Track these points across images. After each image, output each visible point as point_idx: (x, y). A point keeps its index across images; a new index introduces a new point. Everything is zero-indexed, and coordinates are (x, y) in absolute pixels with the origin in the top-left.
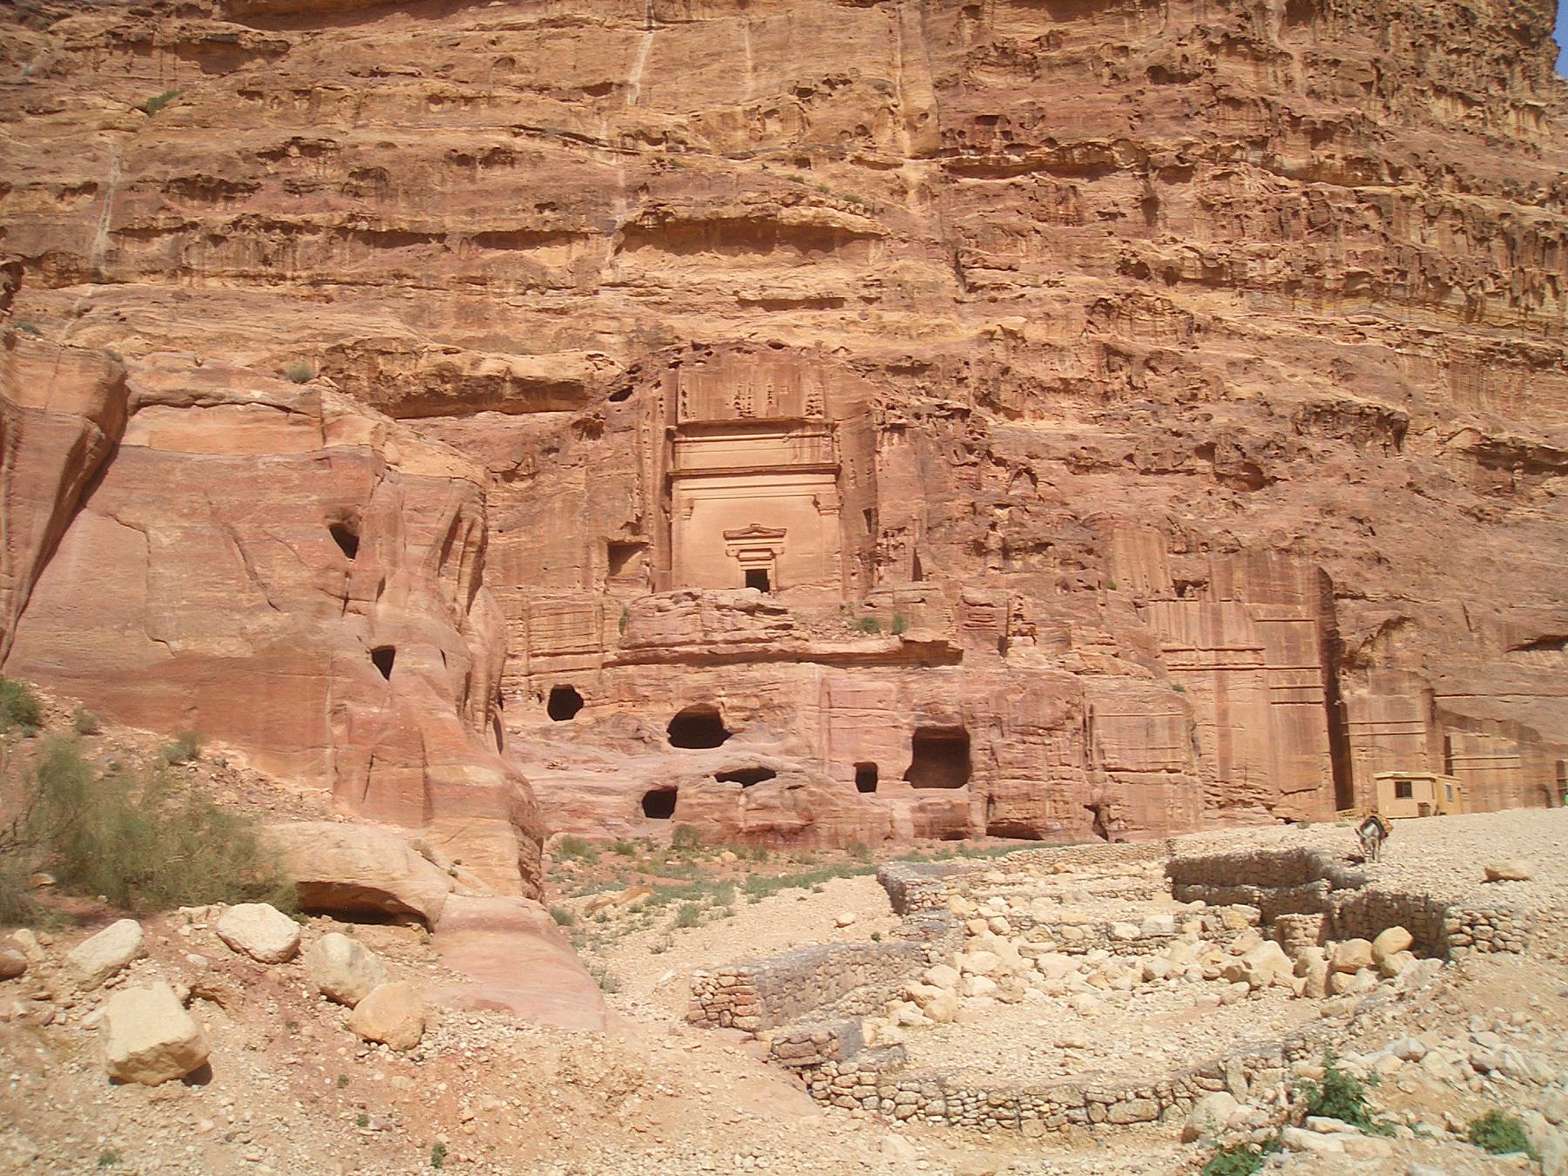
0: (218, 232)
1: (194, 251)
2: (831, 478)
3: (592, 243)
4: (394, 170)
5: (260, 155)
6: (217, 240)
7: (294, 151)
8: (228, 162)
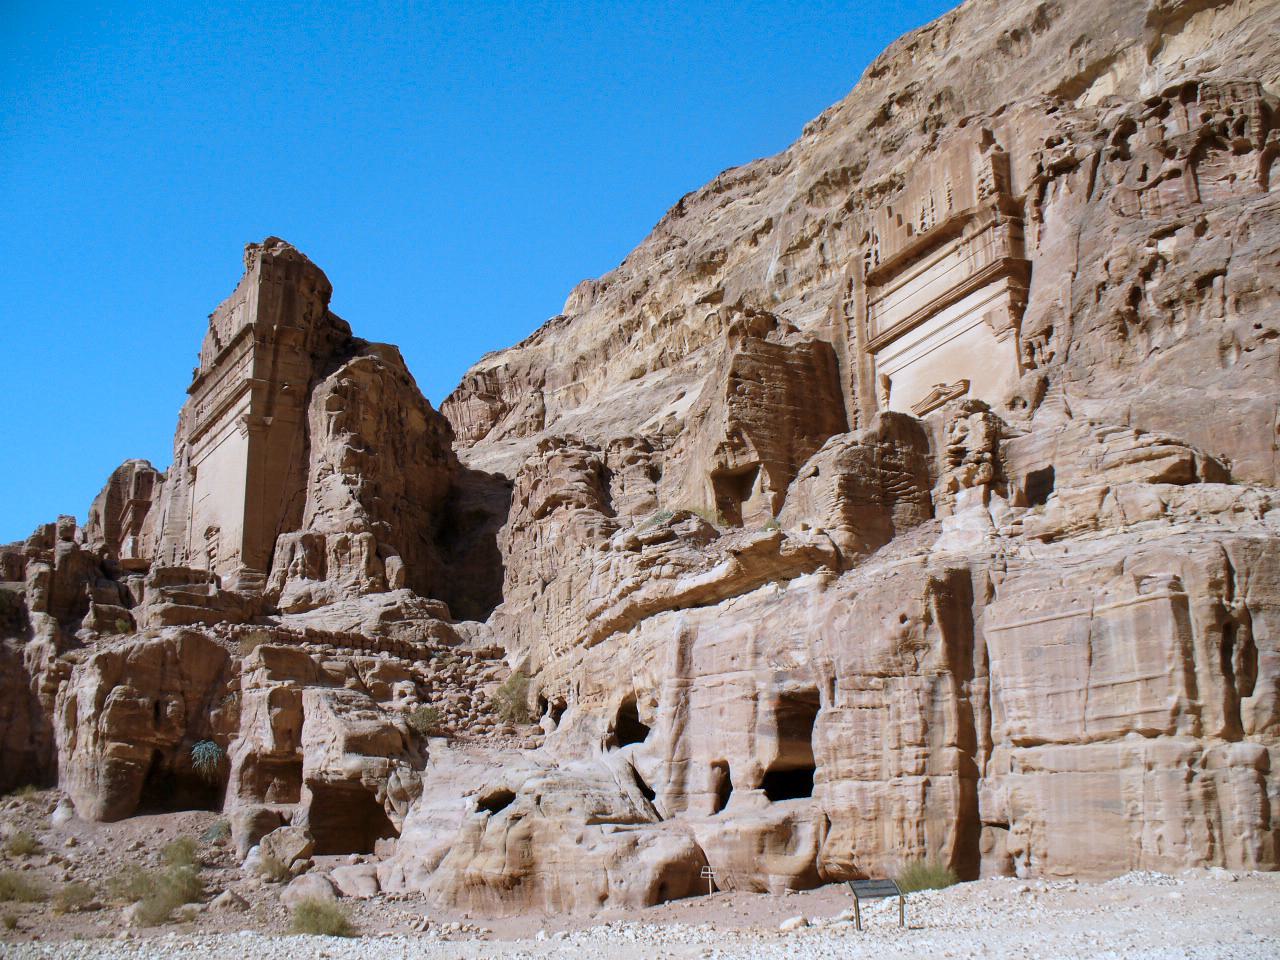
0: (835, 220)
1: (827, 246)
2: (1003, 283)
3: (1130, 58)
4: (956, 85)
5: (869, 128)
6: (838, 226)
7: (895, 109)
8: (848, 149)
